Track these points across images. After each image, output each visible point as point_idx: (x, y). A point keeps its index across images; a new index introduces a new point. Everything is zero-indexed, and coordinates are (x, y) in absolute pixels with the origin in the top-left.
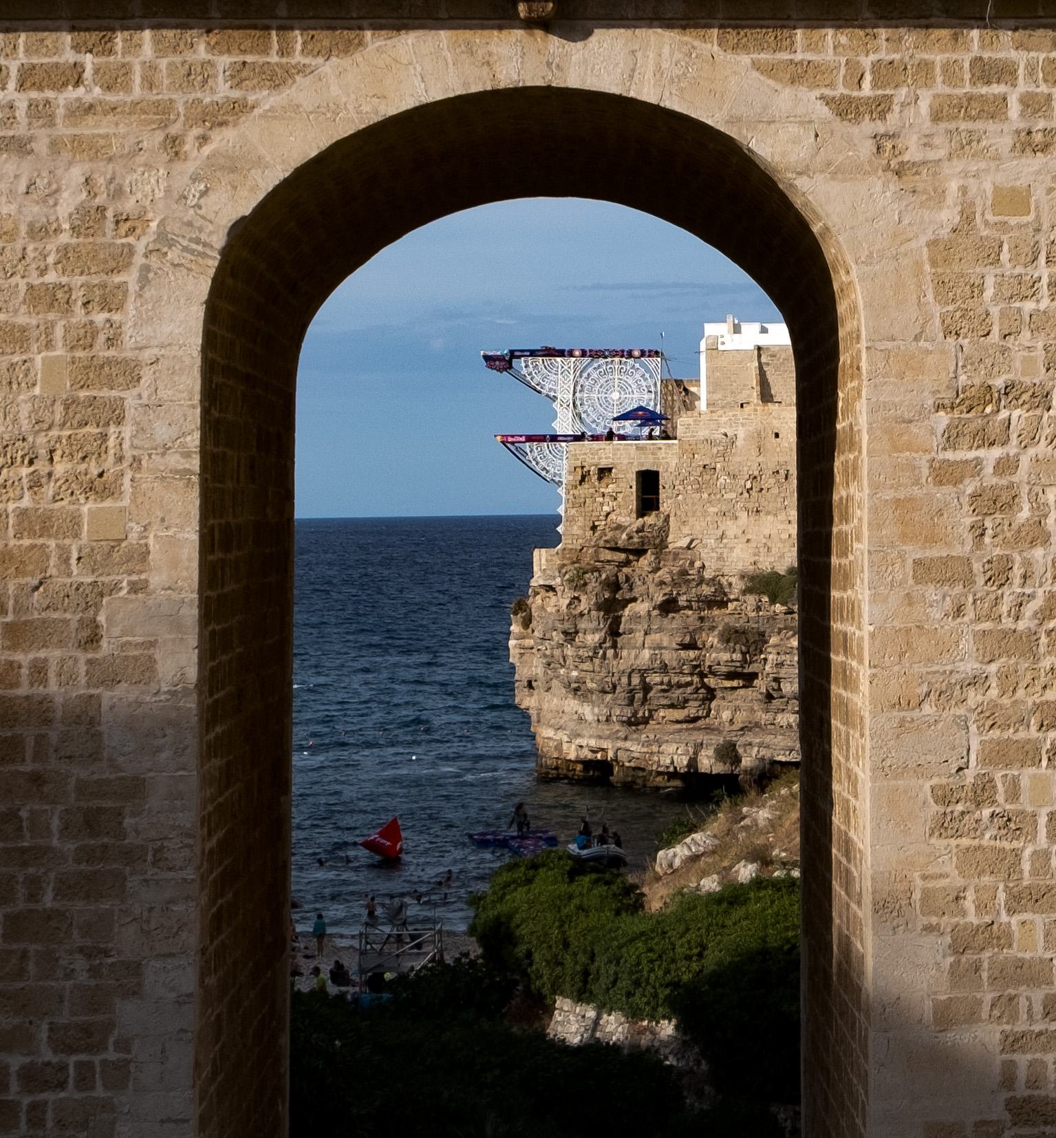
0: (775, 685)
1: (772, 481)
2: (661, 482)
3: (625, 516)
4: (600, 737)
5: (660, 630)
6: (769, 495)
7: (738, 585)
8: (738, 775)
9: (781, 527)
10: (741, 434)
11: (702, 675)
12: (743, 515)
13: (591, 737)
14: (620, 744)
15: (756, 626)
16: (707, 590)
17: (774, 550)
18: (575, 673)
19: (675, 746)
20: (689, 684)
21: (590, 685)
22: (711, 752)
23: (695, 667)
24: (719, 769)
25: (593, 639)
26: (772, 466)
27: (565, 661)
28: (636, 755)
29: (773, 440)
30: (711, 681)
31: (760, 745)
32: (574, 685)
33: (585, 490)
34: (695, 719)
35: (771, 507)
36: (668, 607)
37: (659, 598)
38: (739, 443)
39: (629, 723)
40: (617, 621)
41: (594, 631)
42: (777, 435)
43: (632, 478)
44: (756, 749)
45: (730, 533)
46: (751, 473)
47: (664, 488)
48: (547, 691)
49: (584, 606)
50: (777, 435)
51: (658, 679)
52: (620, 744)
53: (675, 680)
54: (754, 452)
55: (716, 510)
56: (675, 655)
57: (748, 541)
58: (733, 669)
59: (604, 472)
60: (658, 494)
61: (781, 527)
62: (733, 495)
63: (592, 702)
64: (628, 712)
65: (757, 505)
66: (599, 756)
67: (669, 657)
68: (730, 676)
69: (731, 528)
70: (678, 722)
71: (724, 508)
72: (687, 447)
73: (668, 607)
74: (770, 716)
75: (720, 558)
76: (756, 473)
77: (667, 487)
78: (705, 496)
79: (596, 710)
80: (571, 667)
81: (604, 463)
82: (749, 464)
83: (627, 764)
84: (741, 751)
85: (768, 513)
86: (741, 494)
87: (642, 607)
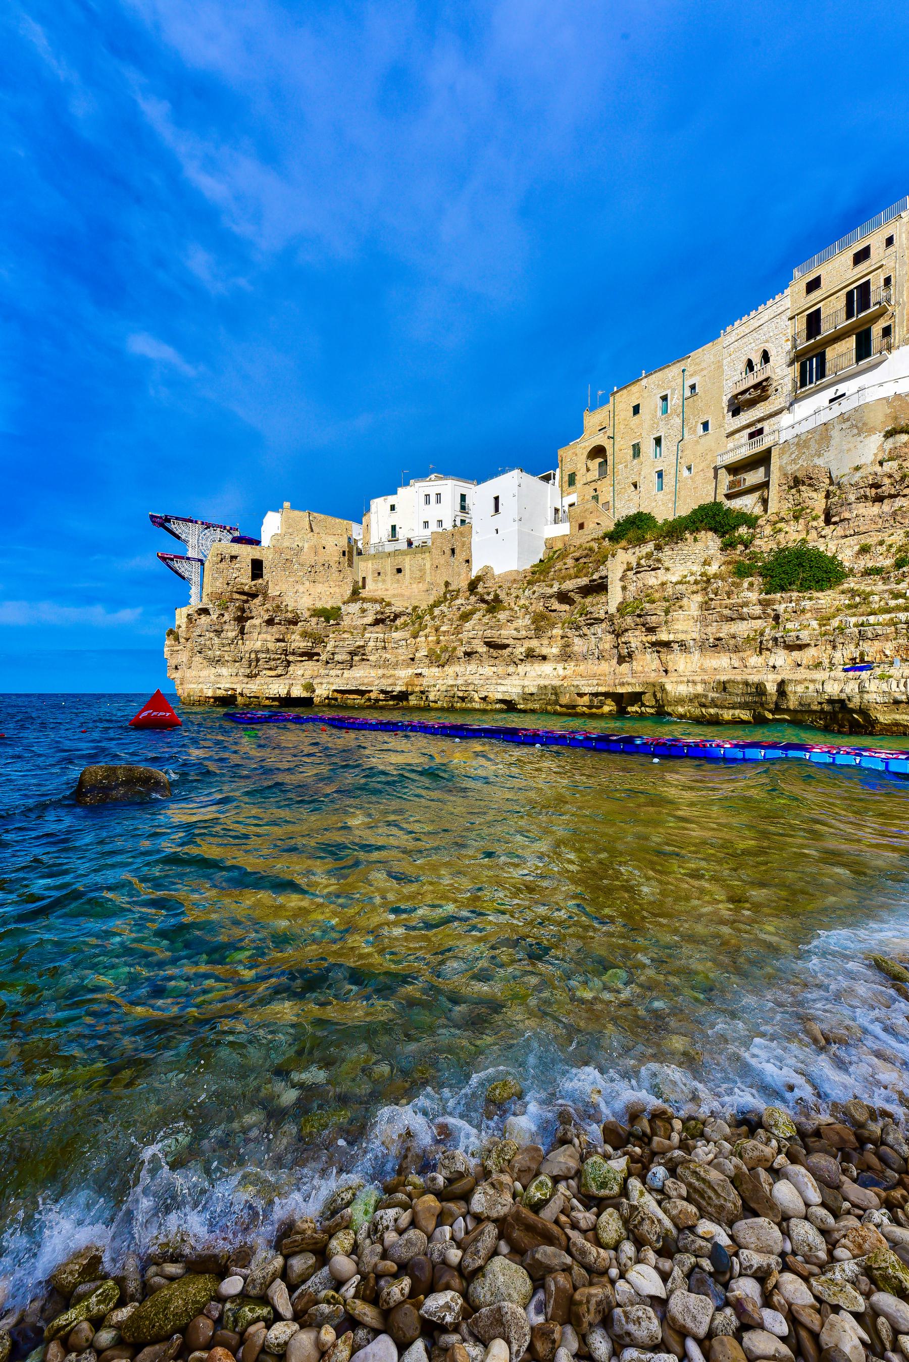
3: (245, 579)
5: (266, 632)
7: (307, 614)
10: (306, 545)
11: (286, 655)
12: (307, 583)
14: (244, 686)
16: (290, 615)
20: (279, 659)
21: (227, 658)
24: (305, 694)
25: (231, 634)
26: (322, 562)
31: (328, 683)
33: (221, 566)
34: (281, 675)
36: (270, 622)
37: (266, 617)
38: (305, 550)
39: (248, 676)
40: (243, 628)
41: (233, 630)
45: (301, 590)
49: (227, 617)
51: (264, 656)
53: (272, 657)
54: (313, 554)
59: (233, 558)
60: (262, 571)
64: (248, 671)
66: (229, 693)
67: (271, 646)
69: (301, 589)
73: (270, 622)
74: (327, 671)
75: (296, 601)
81: (233, 553)
84: (315, 686)
87: (256, 622)
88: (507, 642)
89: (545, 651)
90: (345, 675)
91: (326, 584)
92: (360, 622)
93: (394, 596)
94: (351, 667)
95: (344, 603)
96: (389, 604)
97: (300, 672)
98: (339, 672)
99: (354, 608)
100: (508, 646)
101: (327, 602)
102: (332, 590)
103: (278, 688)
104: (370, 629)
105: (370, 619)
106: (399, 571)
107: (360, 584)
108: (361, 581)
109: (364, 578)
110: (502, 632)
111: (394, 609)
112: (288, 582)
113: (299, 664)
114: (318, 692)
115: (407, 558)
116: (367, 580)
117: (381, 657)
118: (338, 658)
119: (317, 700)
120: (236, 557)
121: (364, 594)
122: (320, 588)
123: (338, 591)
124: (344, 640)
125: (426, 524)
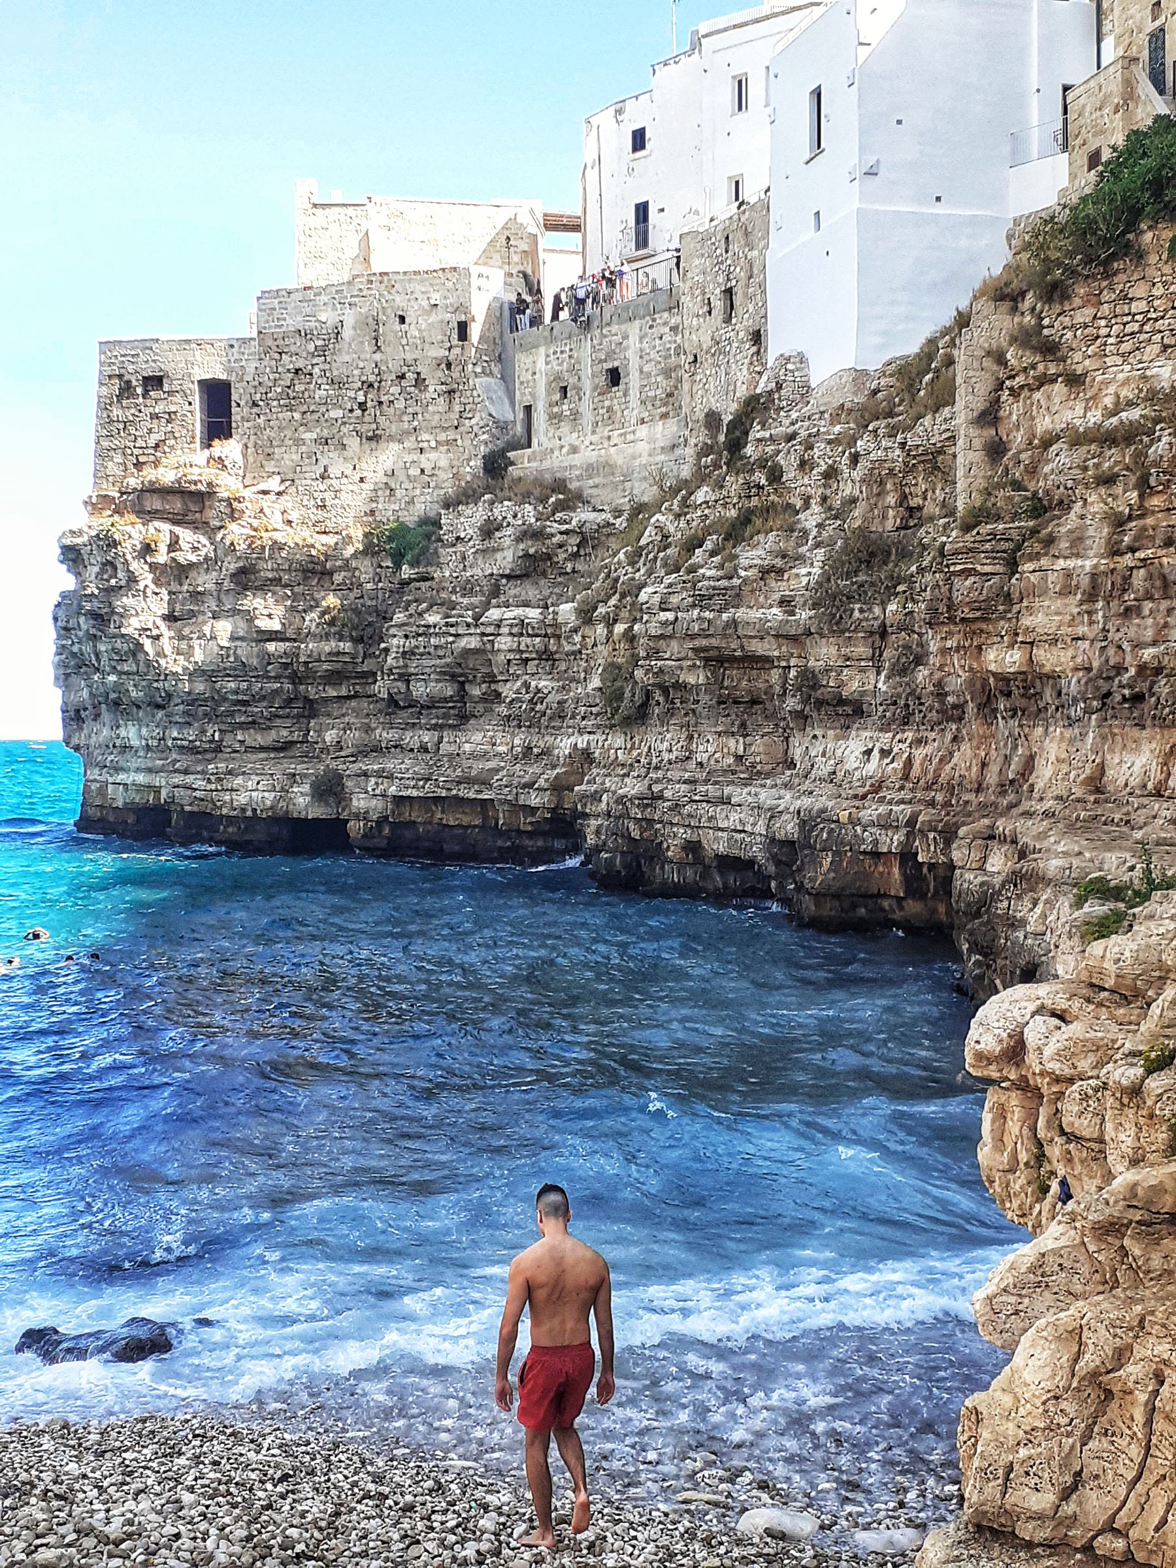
0: (401, 686)
1: (395, 390)
2: (235, 397)
4: (150, 770)
6: (391, 410)
8: (348, 821)
9: (409, 458)
11: (296, 679)
12: (353, 443)
13: (138, 770)
14: (177, 779)
15: (374, 603)
17: (399, 493)
18: (112, 678)
19: (256, 778)
22: (306, 788)
23: (286, 666)
26: (395, 367)
27: (98, 660)
28: (197, 794)
29: (397, 327)
30: (311, 692)
31: (379, 774)
32: (113, 696)
35: (394, 429)
38: (347, 333)
39: (192, 750)
42: (402, 320)
44: (373, 780)
45: (334, 471)
46: (364, 378)
47: (239, 405)
48: (95, 720)
50: (402, 320)
51: (232, 685)
54: (368, 347)
56: (255, 649)
58: (339, 666)
60: (229, 415)
61: (409, 458)
63: (139, 720)
65: (374, 426)
68: (334, 677)
70: (262, 749)
71: (325, 433)
72: (270, 342)
76: (372, 378)
77: (242, 403)
78: (297, 416)
79: (144, 731)
80: (107, 669)
82: (361, 365)
83: (188, 808)
84: (349, 784)
85: (391, 438)
86: (351, 411)
88: (759, 648)
89: (853, 685)
90: (445, 748)
91: (410, 443)
92: (481, 569)
93: (590, 470)
94: (464, 718)
95: (447, 506)
96: (571, 500)
97: (330, 736)
98: (427, 737)
99: (470, 519)
100: (765, 662)
101: (411, 502)
102: (426, 461)
104: (513, 590)
105: (506, 559)
106: (614, 377)
107: (519, 429)
108: (521, 415)
109: (528, 409)
110: (741, 613)
111: (583, 516)
112: (299, 442)
113: (335, 709)
114: (359, 802)
115: (634, 330)
116: (535, 415)
117: (527, 685)
118: (419, 690)
119: (355, 828)
121: (524, 464)
123: (443, 462)
124: (427, 631)
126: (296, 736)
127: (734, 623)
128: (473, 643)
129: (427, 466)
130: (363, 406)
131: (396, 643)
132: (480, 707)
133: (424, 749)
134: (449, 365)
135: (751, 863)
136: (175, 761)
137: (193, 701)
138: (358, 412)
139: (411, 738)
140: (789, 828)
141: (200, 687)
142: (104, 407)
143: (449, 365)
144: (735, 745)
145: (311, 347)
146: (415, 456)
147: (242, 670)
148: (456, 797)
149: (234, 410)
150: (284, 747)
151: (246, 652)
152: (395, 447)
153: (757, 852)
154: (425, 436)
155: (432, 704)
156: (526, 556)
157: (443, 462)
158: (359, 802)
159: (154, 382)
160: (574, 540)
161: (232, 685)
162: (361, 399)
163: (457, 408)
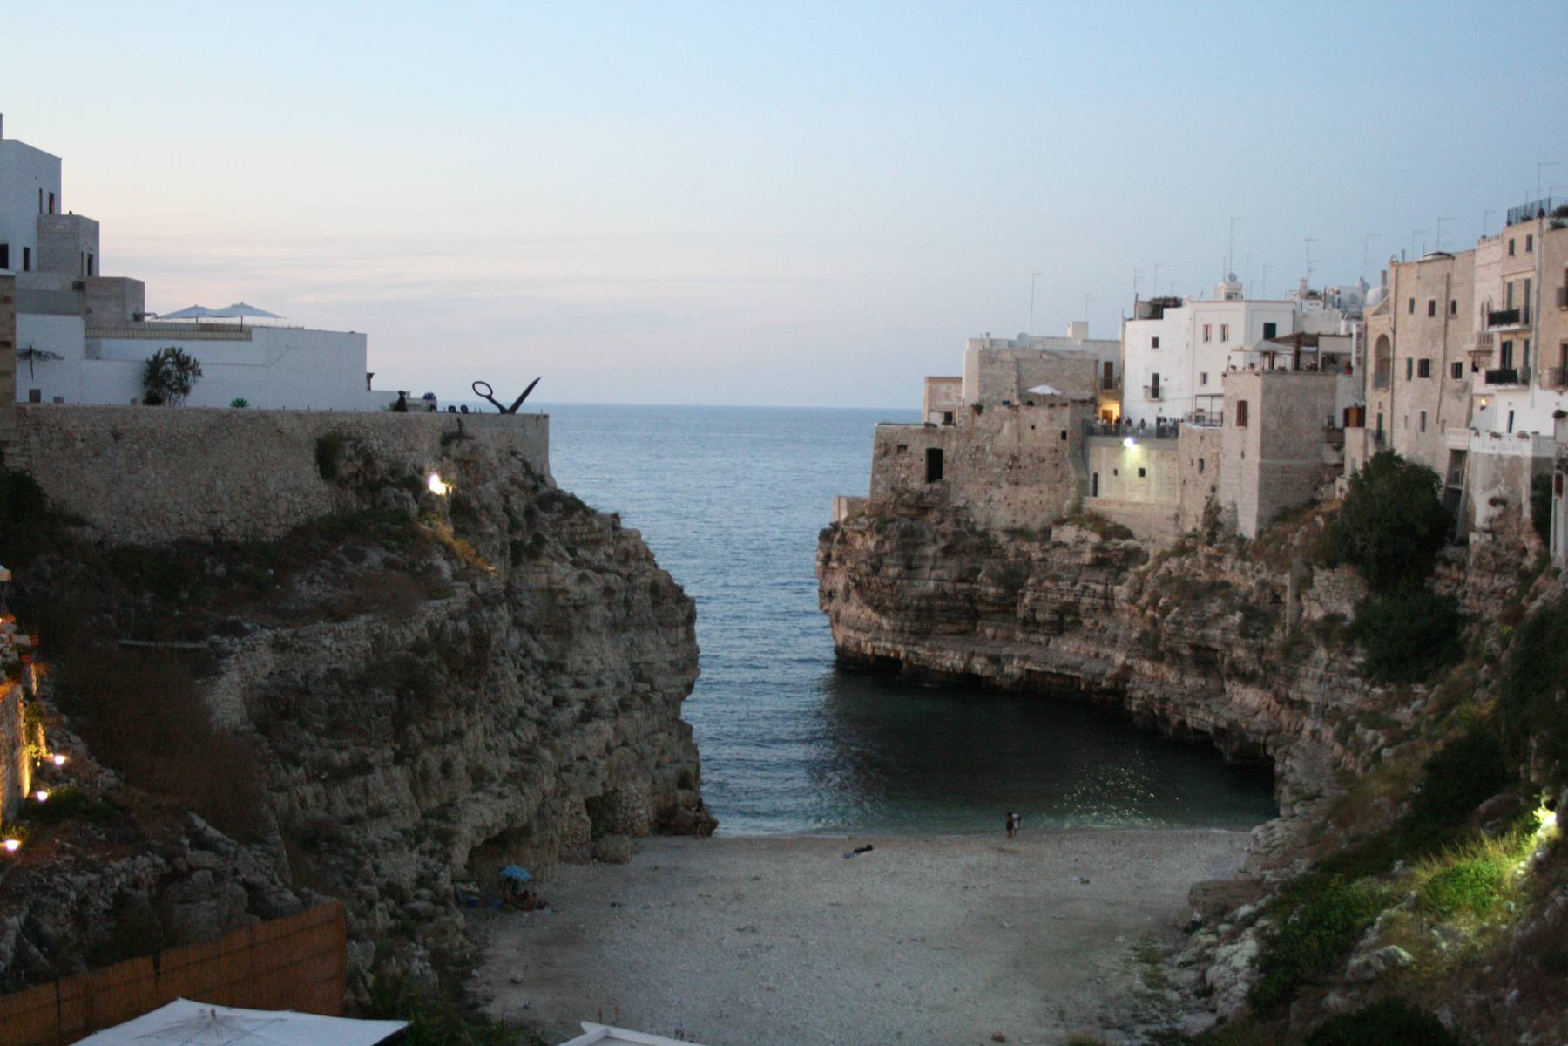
1: (1028, 461)
3: (918, 483)
5: (941, 567)
6: (1026, 471)
9: (1034, 495)
12: (1005, 486)
14: (910, 648)
17: (1028, 513)
25: (892, 572)
30: (980, 607)
32: (875, 603)
33: (886, 461)
35: (1027, 480)
36: (948, 551)
41: (894, 566)
42: (1033, 427)
43: (923, 452)
45: (995, 499)
49: (887, 547)
50: (1033, 427)
52: (910, 648)
55: (985, 480)
57: (1009, 505)
62: (998, 470)
69: (996, 494)
70: (952, 634)
71: (991, 479)
79: (892, 622)
81: (902, 442)
85: (1025, 485)
88: (1214, 645)
90: (1051, 645)
91: (1035, 487)
101: (1035, 517)
102: (1044, 498)
103: (951, 659)
108: (1092, 477)
109: (1096, 476)
110: (1206, 631)
120: (905, 447)
122: (1025, 494)
123: (1052, 499)
124: (1047, 590)
125: (1204, 377)
126: (969, 627)
127: (1203, 636)
128: (1071, 599)
129: (1044, 500)
130: (1011, 468)
131: (1029, 594)
132: (1070, 627)
133: (1040, 643)
134: (1056, 451)
135: (1207, 733)
136: (908, 638)
137: (919, 609)
138: (1008, 470)
139: (1035, 638)
140: (1223, 724)
141: (923, 603)
142: (877, 458)
143: (1056, 451)
144: (1202, 681)
145: (985, 436)
146: (1037, 495)
147: (944, 595)
148: (1061, 674)
149: (944, 464)
150: (960, 633)
151: (948, 587)
152: (1026, 489)
153: (1210, 729)
154: (1043, 485)
155: (1046, 623)
156: (1097, 558)
157: (1052, 499)
158: (1008, 669)
159: (902, 448)
160: (1122, 553)
161: (939, 603)
162: (1010, 463)
163: (1059, 472)
